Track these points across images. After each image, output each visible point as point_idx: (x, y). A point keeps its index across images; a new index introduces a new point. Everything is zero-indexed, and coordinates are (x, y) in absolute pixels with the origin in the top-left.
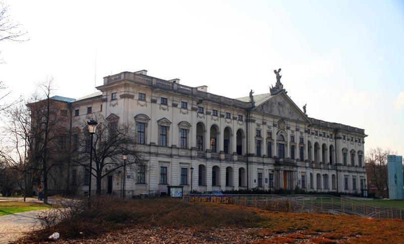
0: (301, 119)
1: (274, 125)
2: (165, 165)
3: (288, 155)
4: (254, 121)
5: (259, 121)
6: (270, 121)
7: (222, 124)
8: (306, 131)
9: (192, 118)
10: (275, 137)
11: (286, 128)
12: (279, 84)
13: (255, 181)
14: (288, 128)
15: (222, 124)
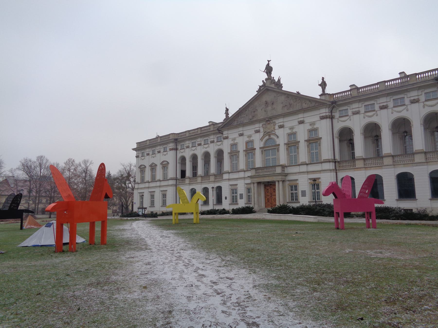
0: (305, 106)
1: (257, 132)
2: (153, 194)
3: (283, 157)
4: (227, 138)
5: (231, 136)
6: (249, 131)
7: (199, 152)
8: (322, 118)
9: (170, 157)
10: (258, 144)
11: (277, 127)
12: (270, 78)
13: (226, 198)
14: (281, 127)
15: (199, 152)
